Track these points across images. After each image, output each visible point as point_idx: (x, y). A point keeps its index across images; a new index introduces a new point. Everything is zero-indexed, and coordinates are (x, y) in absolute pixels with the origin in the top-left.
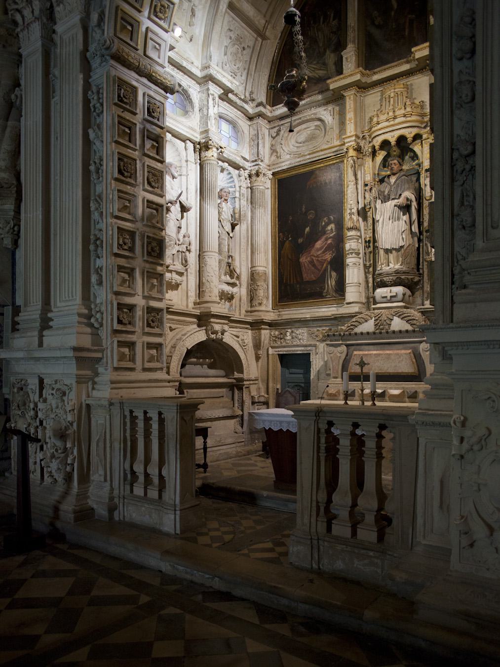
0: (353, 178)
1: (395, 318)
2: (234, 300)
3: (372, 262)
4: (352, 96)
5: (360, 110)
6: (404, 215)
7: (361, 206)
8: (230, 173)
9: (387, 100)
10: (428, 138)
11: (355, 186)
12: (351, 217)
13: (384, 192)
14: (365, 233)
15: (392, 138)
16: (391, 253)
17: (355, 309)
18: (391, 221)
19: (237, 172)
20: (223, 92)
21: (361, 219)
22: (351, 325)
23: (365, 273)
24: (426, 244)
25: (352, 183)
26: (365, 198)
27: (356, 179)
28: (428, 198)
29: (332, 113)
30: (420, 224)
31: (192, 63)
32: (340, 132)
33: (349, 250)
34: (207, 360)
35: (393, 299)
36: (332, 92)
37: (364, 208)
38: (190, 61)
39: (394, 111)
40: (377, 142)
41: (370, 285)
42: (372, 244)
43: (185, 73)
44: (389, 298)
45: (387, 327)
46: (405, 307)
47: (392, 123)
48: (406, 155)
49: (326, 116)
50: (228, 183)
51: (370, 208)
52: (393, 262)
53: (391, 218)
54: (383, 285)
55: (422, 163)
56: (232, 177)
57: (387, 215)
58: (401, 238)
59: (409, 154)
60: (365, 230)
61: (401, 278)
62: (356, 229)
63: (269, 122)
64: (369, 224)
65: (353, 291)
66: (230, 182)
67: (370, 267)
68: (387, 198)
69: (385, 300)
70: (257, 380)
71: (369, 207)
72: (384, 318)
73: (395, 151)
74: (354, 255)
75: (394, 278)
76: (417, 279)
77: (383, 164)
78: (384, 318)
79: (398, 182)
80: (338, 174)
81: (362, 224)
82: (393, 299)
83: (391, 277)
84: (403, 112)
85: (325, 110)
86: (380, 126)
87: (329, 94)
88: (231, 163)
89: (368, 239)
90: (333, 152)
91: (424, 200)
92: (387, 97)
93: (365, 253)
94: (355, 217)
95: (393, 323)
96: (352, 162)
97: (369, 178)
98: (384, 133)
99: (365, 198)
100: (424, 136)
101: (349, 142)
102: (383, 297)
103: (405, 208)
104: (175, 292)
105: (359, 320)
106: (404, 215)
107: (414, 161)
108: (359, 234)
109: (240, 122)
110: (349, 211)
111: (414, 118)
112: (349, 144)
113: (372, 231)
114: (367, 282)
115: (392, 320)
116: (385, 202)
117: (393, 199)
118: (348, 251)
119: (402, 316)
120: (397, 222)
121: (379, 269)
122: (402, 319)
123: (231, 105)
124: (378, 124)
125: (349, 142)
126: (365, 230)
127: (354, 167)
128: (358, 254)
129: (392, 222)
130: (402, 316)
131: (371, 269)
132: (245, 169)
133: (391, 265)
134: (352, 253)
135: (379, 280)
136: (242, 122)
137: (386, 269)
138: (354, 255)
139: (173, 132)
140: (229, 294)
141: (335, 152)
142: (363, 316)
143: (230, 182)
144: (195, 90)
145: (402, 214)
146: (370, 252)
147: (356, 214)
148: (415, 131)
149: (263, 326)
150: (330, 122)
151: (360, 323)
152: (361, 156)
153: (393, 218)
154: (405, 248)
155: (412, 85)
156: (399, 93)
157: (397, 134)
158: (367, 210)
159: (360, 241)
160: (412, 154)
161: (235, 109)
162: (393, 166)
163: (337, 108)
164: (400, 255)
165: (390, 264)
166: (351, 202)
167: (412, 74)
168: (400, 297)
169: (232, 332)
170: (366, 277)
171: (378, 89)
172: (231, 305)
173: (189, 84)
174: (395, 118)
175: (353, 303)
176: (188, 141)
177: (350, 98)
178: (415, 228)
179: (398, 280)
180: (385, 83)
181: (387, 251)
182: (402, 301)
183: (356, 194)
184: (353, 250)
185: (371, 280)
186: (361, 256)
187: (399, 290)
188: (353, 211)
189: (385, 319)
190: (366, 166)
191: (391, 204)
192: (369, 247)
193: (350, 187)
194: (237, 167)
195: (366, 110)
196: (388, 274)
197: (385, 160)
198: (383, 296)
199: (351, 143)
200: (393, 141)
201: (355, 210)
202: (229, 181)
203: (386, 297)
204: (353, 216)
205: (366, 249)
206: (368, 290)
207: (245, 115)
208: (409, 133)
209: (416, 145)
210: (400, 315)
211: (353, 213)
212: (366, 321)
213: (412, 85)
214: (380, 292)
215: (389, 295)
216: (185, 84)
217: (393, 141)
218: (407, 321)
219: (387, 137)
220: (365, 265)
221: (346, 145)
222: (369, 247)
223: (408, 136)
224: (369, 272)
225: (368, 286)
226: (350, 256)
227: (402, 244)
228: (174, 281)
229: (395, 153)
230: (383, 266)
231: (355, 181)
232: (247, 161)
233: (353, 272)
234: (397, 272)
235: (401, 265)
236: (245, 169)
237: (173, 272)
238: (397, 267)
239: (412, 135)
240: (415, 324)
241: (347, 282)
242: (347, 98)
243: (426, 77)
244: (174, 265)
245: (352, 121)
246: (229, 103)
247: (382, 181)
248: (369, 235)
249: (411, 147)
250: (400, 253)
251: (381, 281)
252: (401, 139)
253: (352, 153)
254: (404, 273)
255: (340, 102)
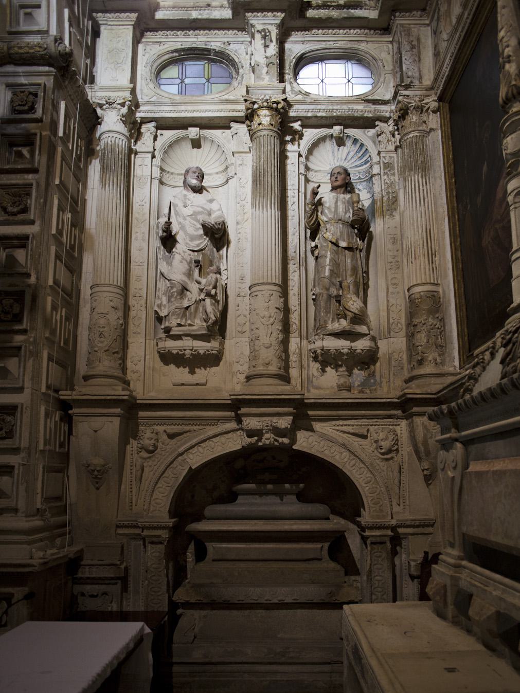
2: (378, 364)
8: (355, 141)
19: (372, 132)
20: (283, 15)
31: (209, 5)
34: (287, 486)
38: (201, 4)
43: (210, 29)
50: (360, 158)
56: (362, 145)
63: (424, 10)
66: (363, 155)
70: (432, 526)
88: (348, 122)
104: (214, 369)
109: (363, 46)
123: (329, 28)
132: (385, 120)
136: (370, 45)
139: (199, 122)
140: (343, 354)
143: (363, 155)
144: (242, 42)
149: (415, 409)
161: (341, 31)
169: (340, 428)
172: (373, 375)
173: (226, 40)
176: (232, 124)
194: (367, 123)
202: (361, 153)
207: (370, 29)
216: (219, 44)
228: (188, 352)
232: (385, 103)
236: (385, 120)
237: (184, 338)
244: (190, 325)
246: (323, 28)
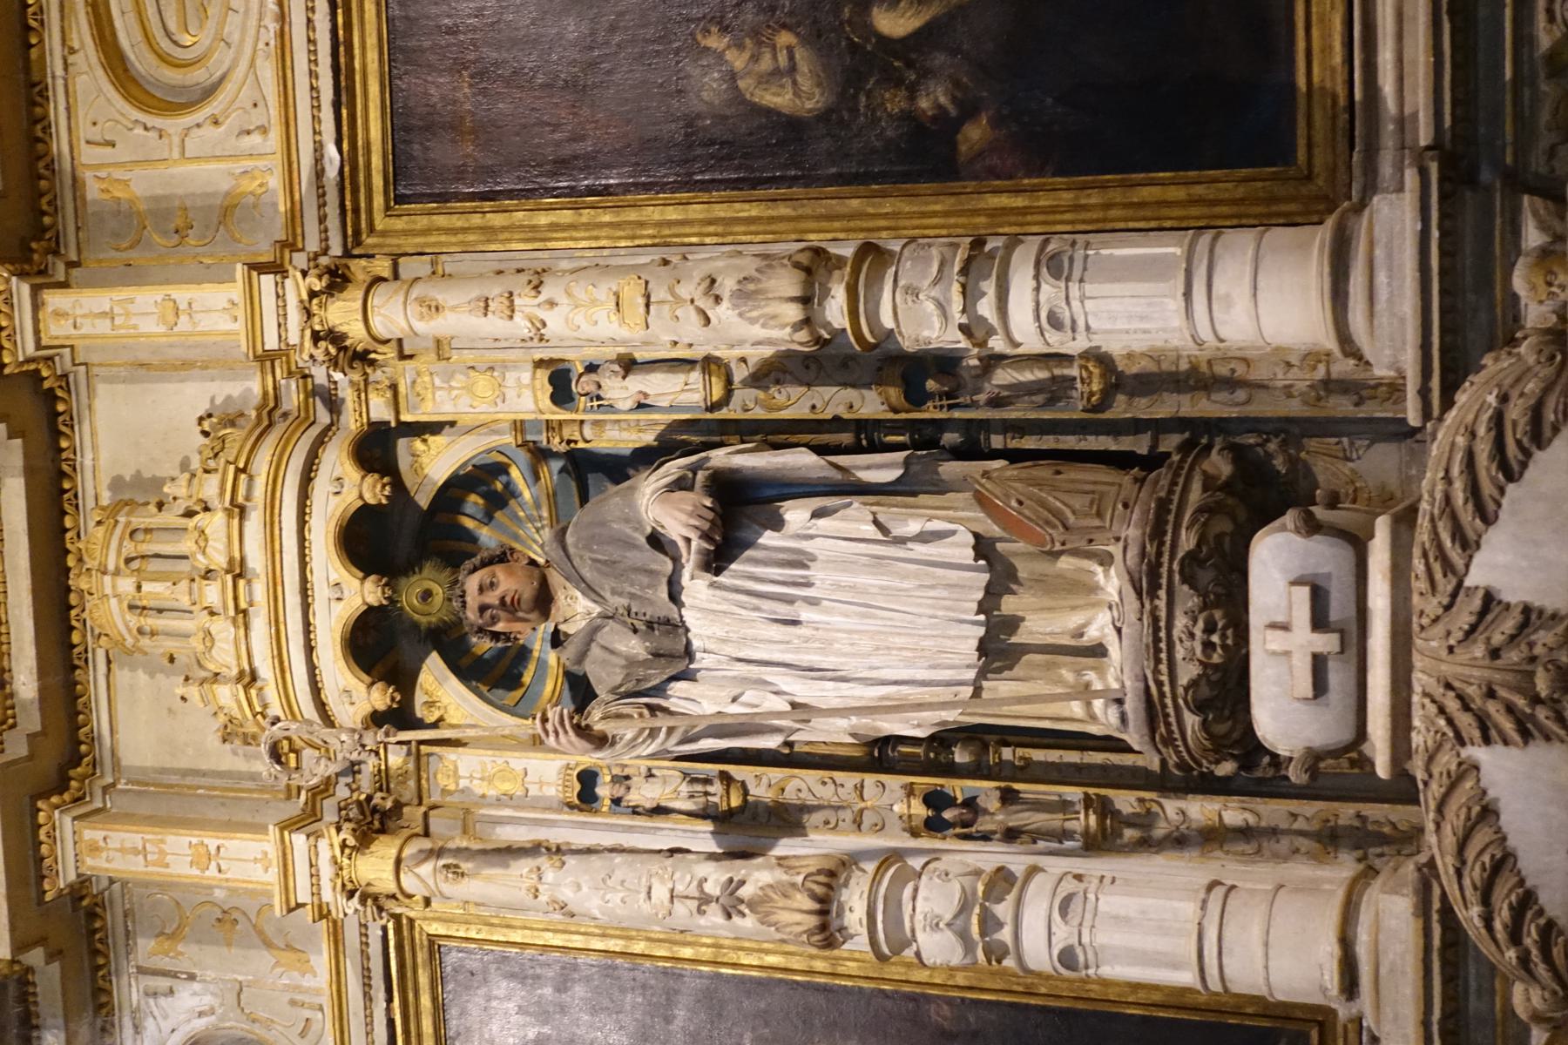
0: (523, 866)
1: (1478, 576)
3: (1074, 793)
4: (91, 834)
5: (177, 798)
6: (777, 524)
7: (702, 838)
9: (151, 622)
10: (394, 387)
11: (571, 861)
12: (753, 905)
13: (632, 663)
14: (879, 828)
15: (343, 594)
16: (1013, 623)
17: (1392, 916)
18: (805, 614)
21: (785, 847)
22: (1515, 937)
23: (1146, 844)
24: (996, 402)
25: (550, 876)
26: (659, 811)
27: (535, 849)
28: (717, 392)
29: (162, 983)
30: (868, 437)
32: (268, 944)
33: (964, 936)
35: (1335, 615)
36: (35, 957)
37: (722, 819)
39: (208, 574)
40: (355, 695)
41: (1233, 813)
42: (958, 770)
44: (1326, 643)
45: (1544, 638)
46: (1405, 520)
47: (260, 590)
48: (472, 539)
49: (166, 1026)
51: (726, 778)
52: (1074, 620)
53: (783, 610)
54: (1227, 688)
55: (519, 426)
57: (769, 641)
58: (920, 550)
59: (469, 523)
60: (858, 823)
61: (1191, 556)
62: (833, 875)
64: (826, 793)
65: (1256, 931)
67: (1105, 809)
68: (667, 644)
69: (1338, 677)
71: (717, 788)
72: (1470, 667)
73: (427, 595)
74: (1003, 910)
75: (1187, 599)
76: (1220, 464)
77: (494, 686)
78: (1470, 667)
79: (587, 573)
80: (502, 987)
81: (811, 847)
82: (1341, 607)
83: (1181, 622)
84: (215, 523)
85: (137, 1029)
86: (266, 670)
87: (48, 977)
89: (920, 810)
90: (368, 997)
91: (723, 414)
92: (134, 620)
93: (1011, 835)
94: (758, 876)
95: (1514, 592)
96: (426, 869)
97: (549, 772)
98: (309, 649)
99: (659, 811)
100: (380, 410)
101: (315, 876)
102: (1320, 686)
103: (737, 514)
105: (1474, 874)
106: (777, 524)
107: (511, 492)
108: (870, 867)
110: (714, 916)
111: (262, 464)
112: (326, 871)
113: (870, 779)
114: (1213, 837)
115: (1489, 599)
116: (688, 653)
117: (675, 597)
118: (969, 946)
119: (1467, 516)
120: (815, 573)
121: (1113, 715)
122: (1488, 519)
124: (250, 678)
125: (315, 876)
126: (858, 823)
127: (452, 859)
128: (1002, 881)
129: (813, 602)
130: (1467, 516)
131: (1125, 801)
133: (1099, 627)
134: (989, 923)
135: (1191, 720)
137: (1119, 669)
138: (1003, 910)
141: (367, 986)
142: (1450, 841)
145: (768, 538)
146: (1008, 797)
147: (739, 869)
148: (336, 461)
150: (207, 1001)
151: (1504, 862)
152: (413, 814)
153: (789, 600)
154: (994, 530)
155: (117, 484)
156: (129, 548)
157: (327, 564)
158: (735, 801)
159: (916, 863)
160: (474, 501)
162: (492, 598)
163: (146, 948)
164: (1043, 567)
165: (1092, 634)
166: (661, 893)
167: (63, 475)
168: (1325, 556)
170: (1179, 841)
171: (96, 680)
174: (238, 571)
175: (1346, 943)
177: (94, 849)
178: (880, 469)
179: (1206, 576)
180: (76, 638)
181: (998, 649)
182: (1358, 544)
183: (618, 859)
184: (964, 908)
185: (1200, 810)
186: (1016, 860)
187: (1276, 562)
188: (712, 888)
189: (1479, 651)
190: (479, 788)
191: (706, 608)
192: (970, 803)
193: (567, 894)
195: (183, 763)
196: (1158, 645)
197: (470, 671)
198: (1305, 686)
199: (320, 857)
200: (363, 593)
201: (715, 877)
203: (1319, 663)
204: (746, 892)
205: (984, 824)
206: (1274, 832)
208: (343, 487)
209: (417, 469)
210: (1458, 534)
211: (733, 886)
212: (1488, 812)
213: (117, 484)
214: (1282, 715)
215: (1305, 640)
217: (363, 593)
218: (1511, 475)
219: (331, 623)
220: (1095, 844)
221: (327, 895)
222: (970, 803)
223: (349, 500)
224: (1144, 821)
225: (1245, 833)
226: (1005, 935)
227: (961, 549)
229: (439, 593)
230: (1097, 686)
231: (543, 861)
233: (1120, 921)
234: (1146, 582)
235: (1106, 560)
238: (1112, 583)
239: (352, 473)
240: (1536, 413)
241: (1186, 978)
242: (91, 864)
243: (98, 404)
245: (212, 843)
247: (581, 690)
248: (893, 797)
249: (424, 501)
250: (1024, 570)
251: (1199, 707)
252: (365, 540)
253: (375, 867)
254: (1157, 533)
255: (113, 919)
